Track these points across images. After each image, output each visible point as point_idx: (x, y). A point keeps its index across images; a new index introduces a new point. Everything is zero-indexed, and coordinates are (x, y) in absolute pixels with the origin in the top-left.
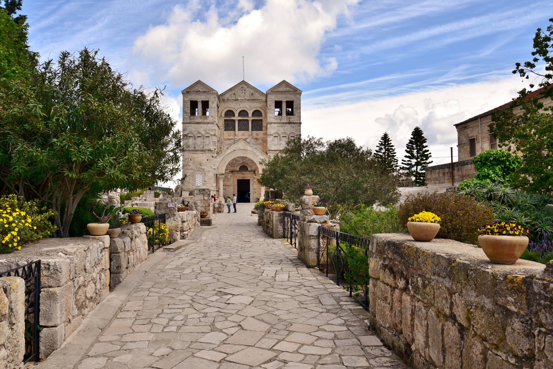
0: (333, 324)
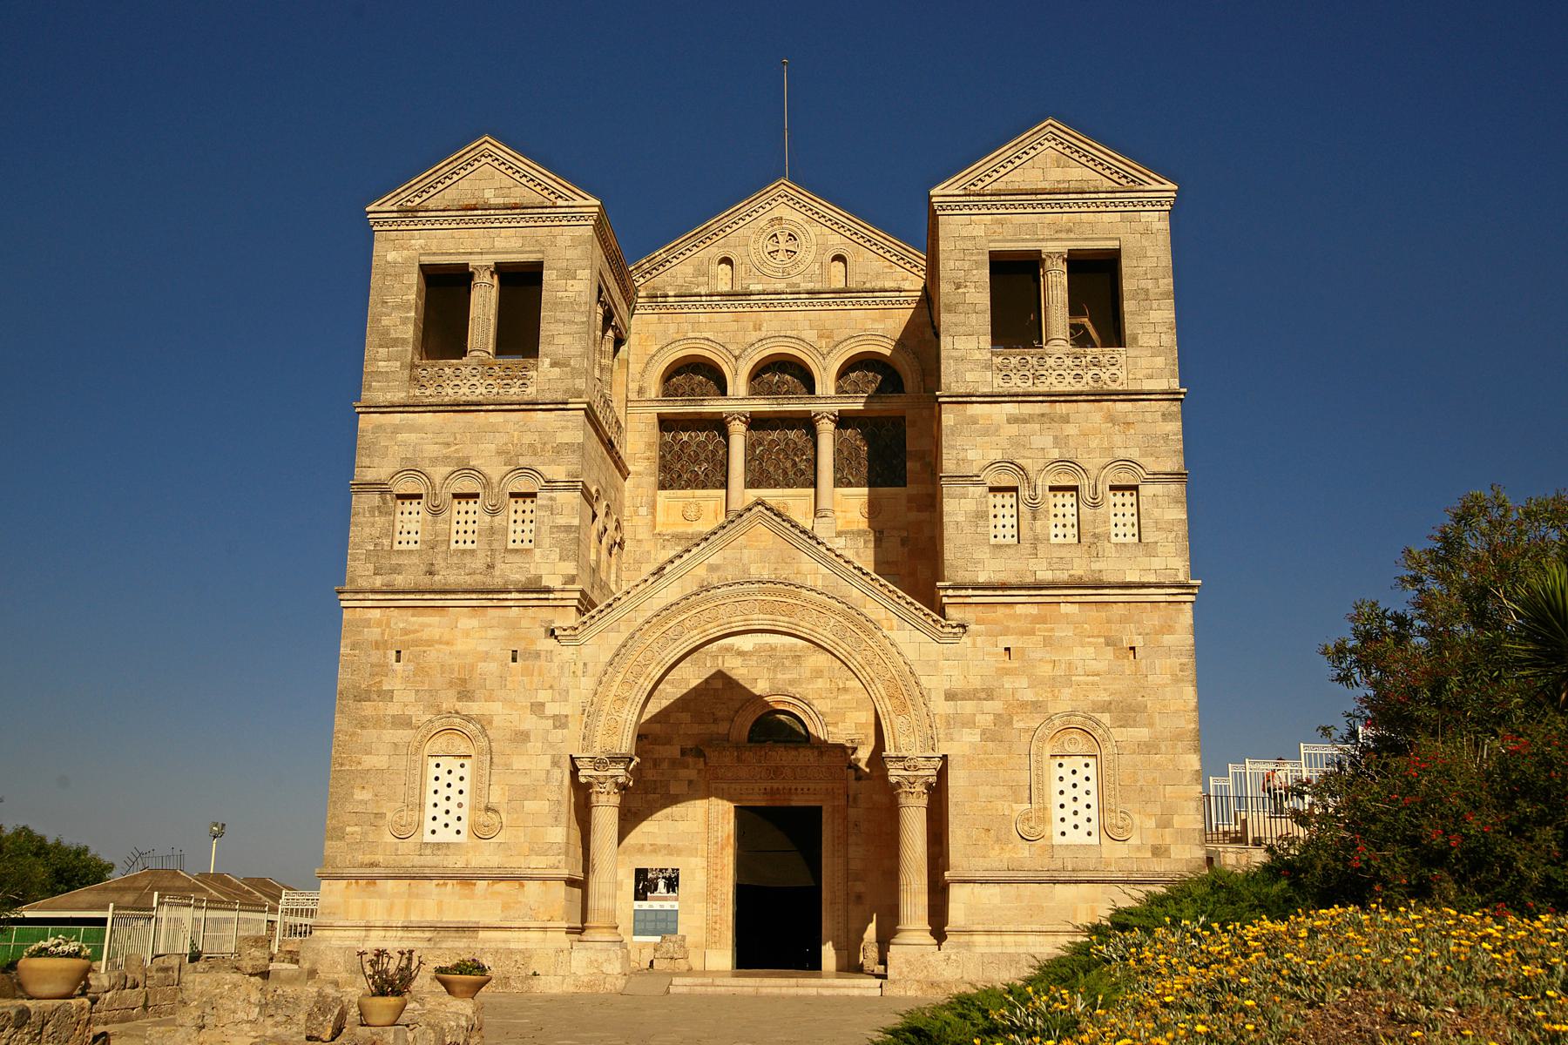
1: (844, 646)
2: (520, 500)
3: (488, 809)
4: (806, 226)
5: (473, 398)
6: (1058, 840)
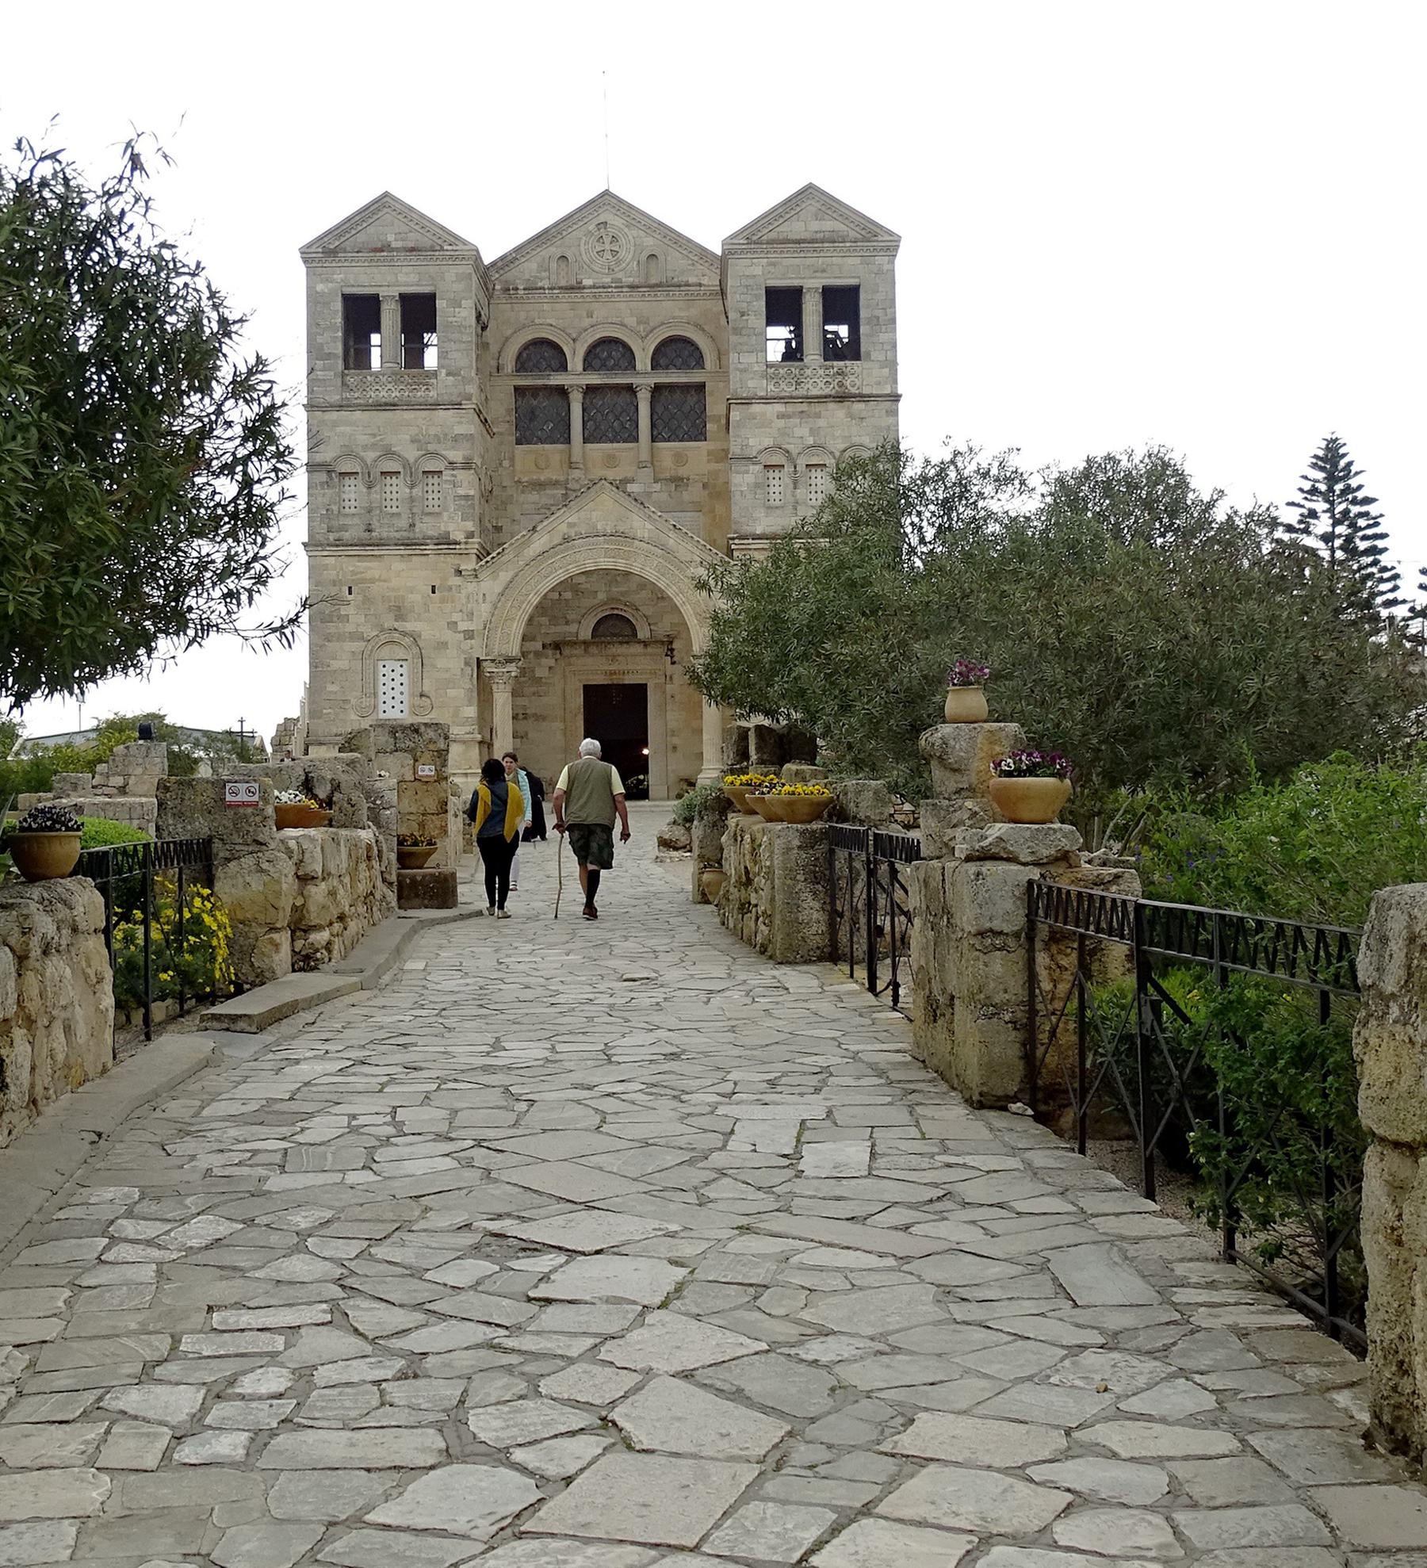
0: (1150, 1418)
3: (421, 696)
4: (626, 230)
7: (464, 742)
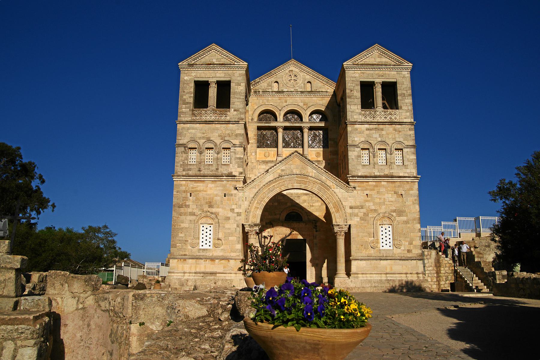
1: (321, 193)
2: (225, 150)
3: (218, 239)
4: (299, 73)
5: (211, 120)
6: (381, 248)
7: (235, 259)
